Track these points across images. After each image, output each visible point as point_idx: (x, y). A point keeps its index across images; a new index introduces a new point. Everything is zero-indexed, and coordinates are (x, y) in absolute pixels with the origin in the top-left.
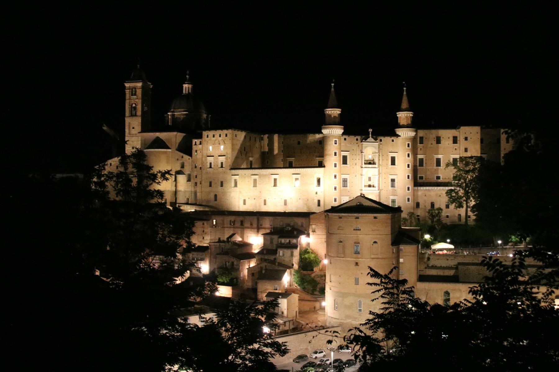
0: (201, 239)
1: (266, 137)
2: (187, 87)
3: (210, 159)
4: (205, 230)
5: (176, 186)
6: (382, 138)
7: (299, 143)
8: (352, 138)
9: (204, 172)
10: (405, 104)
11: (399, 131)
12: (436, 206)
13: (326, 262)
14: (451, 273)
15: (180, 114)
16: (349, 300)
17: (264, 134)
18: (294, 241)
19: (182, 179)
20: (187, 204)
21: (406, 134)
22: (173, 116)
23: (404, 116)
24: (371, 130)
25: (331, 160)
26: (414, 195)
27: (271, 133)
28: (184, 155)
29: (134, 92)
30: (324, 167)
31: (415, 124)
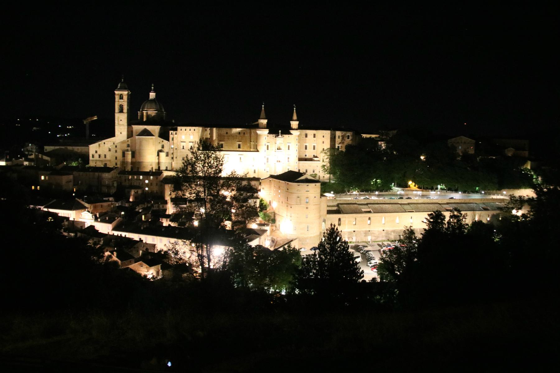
1: (208, 129)
2: (152, 95)
3: (183, 144)
5: (159, 159)
7: (227, 133)
8: (271, 135)
9: (179, 151)
10: (295, 117)
11: (292, 132)
14: (335, 208)
15: (152, 112)
17: (208, 127)
20: (166, 170)
21: (295, 133)
22: (147, 113)
23: (294, 124)
24: (280, 131)
25: (262, 147)
26: (299, 167)
27: (211, 126)
29: (122, 98)
30: (258, 151)
31: (300, 127)
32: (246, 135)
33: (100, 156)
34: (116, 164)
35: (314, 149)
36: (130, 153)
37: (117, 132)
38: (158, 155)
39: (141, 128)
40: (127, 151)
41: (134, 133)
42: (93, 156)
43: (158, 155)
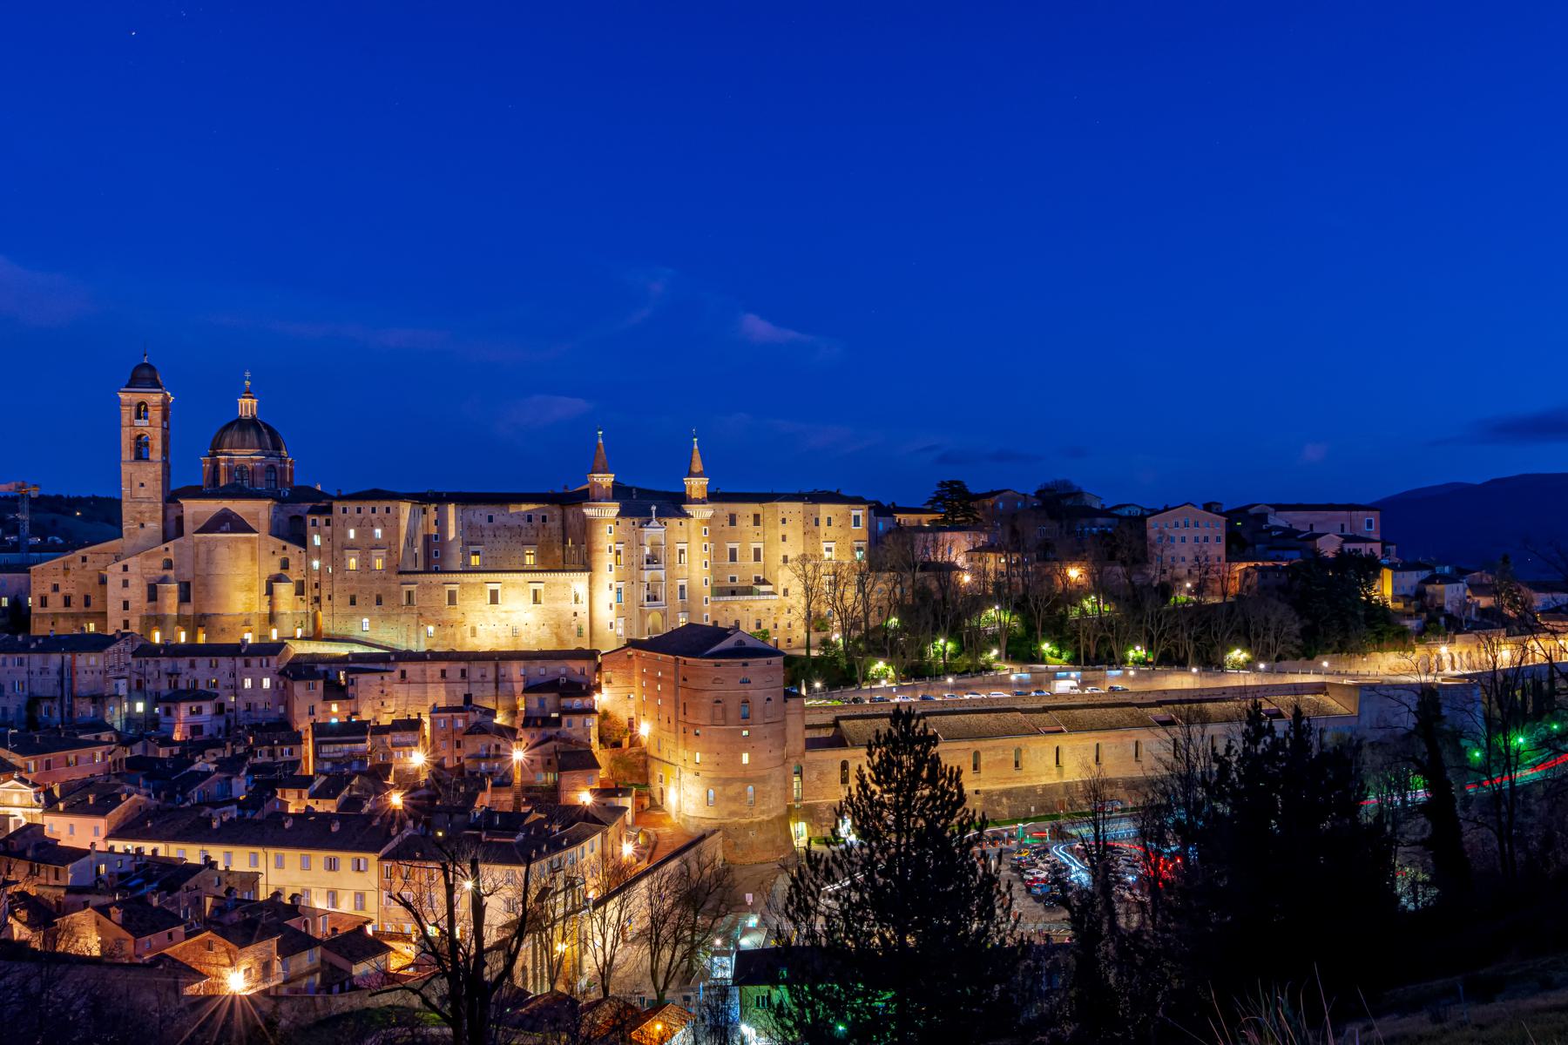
0: (378, 706)
1: (432, 508)
4: (387, 690)
6: (667, 520)
10: (697, 466)
11: (689, 509)
12: (764, 627)
13: (645, 729)
14: (830, 732)
16: (732, 790)
18: (587, 702)
19: (285, 591)
21: (701, 512)
23: (696, 485)
24: (654, 508)
28: (288, 545)
31: (714, 497)
32: (550, 524)
33: (67, 601)
34: (126, 624)
35: (757, 558)
36: (175, 586)
37: (128, 525)
38: (270, 591)
39: (212, 507)
40: (164, 580)
41: (188, 526)
42: (44, 602)
43: (270, 591)
